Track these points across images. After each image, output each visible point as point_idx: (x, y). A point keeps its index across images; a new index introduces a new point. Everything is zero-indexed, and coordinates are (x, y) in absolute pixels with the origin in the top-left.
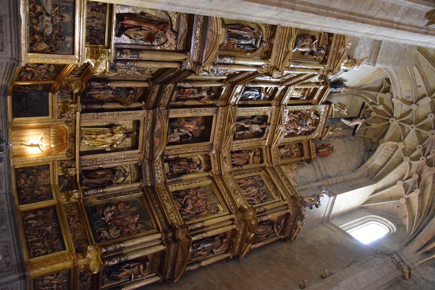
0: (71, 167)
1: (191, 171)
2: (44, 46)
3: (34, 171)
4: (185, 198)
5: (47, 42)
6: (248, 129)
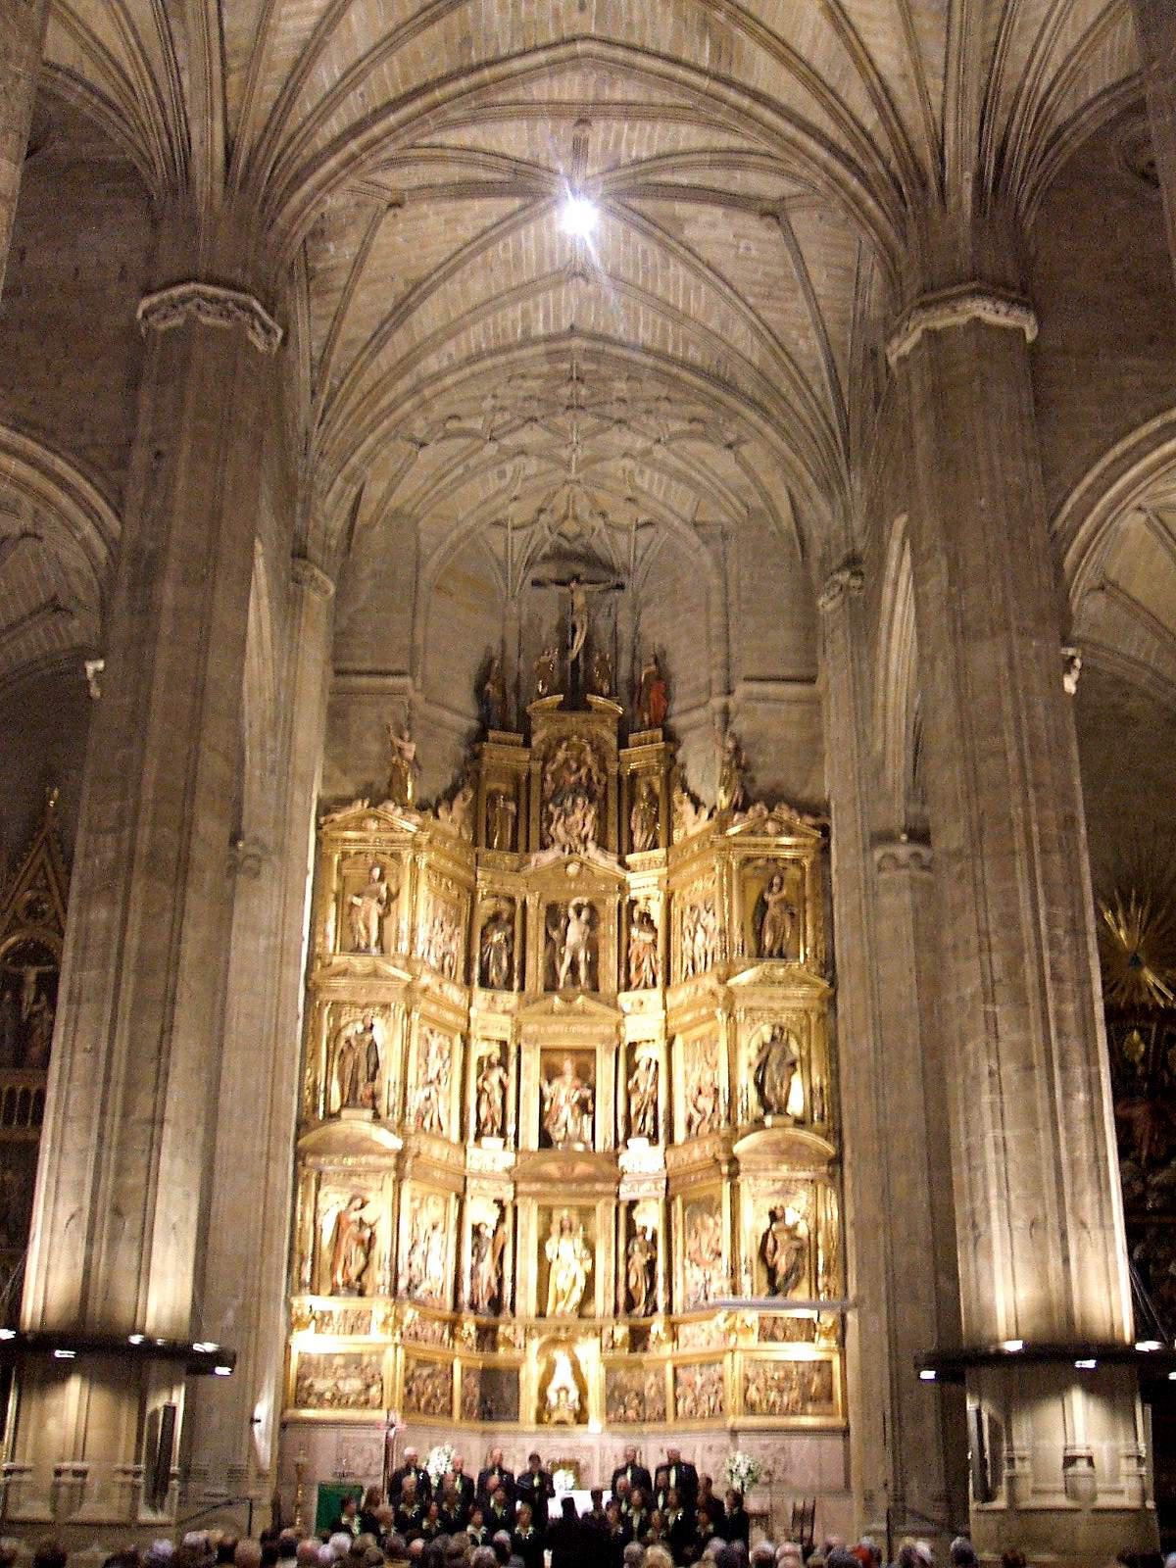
2: (374, 1391)
5: (368, 1387)
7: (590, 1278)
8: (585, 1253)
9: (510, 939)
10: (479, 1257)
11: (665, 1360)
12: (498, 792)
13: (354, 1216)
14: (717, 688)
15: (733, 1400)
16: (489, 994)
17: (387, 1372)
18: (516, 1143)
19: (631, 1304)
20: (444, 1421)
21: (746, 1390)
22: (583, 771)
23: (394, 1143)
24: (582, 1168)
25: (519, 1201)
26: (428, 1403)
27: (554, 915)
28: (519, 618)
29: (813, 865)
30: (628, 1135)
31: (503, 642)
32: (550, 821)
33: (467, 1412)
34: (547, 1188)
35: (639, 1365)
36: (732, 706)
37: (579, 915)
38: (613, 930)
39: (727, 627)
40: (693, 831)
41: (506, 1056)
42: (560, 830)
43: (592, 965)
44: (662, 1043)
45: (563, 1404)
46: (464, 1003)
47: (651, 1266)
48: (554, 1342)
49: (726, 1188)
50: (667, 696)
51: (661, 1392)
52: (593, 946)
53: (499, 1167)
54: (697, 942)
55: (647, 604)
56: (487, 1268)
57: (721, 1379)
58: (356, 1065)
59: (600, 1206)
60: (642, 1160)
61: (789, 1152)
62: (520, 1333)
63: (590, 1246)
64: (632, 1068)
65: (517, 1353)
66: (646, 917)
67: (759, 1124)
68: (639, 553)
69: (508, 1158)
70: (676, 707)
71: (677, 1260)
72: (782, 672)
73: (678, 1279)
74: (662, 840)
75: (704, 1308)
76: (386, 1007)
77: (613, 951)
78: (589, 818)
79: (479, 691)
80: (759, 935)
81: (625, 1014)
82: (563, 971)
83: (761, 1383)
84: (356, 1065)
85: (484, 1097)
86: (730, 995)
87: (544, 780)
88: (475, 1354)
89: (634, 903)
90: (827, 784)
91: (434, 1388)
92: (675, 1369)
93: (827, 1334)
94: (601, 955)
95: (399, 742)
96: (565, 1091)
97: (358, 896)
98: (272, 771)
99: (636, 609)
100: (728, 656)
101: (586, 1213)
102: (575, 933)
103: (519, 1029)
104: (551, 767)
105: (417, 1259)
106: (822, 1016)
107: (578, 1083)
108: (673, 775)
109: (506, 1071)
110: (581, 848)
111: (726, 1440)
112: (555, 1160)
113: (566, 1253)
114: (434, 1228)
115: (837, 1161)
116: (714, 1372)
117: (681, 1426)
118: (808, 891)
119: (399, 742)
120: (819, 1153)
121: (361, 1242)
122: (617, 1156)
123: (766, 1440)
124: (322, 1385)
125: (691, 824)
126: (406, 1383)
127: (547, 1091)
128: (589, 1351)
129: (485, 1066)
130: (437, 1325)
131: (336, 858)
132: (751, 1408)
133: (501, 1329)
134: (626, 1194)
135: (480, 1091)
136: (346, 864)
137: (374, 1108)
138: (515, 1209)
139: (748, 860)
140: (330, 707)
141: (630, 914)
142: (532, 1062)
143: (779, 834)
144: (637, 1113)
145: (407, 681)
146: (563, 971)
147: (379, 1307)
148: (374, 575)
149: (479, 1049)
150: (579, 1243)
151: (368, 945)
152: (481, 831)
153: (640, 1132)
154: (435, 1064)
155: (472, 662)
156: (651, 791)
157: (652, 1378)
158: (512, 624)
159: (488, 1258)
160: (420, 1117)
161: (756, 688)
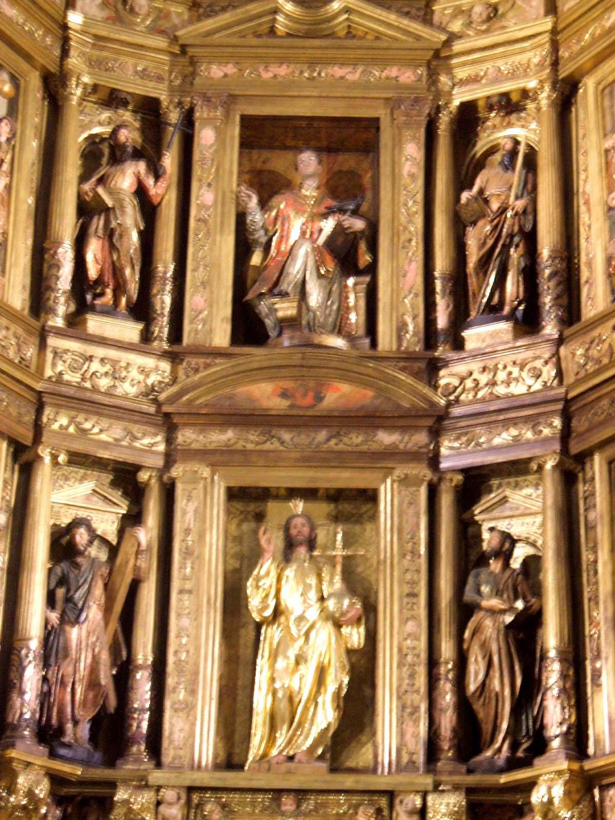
1: (520, 204)
7: (363, 667)
8: (349, 605)
10: (63, 601)
18: (176, 334)
19: (470, 736)
24: (340, 394)
25: (177, 471)
30: (460, 319)
34: (251, 439)
44: (545, 97)
47: (525, 630)
56: (88, 636)
59: (386, 493)
60: (498, 364)
85: (98, 223)
96: (300, 231)
101: (355, 505)
103: (189, 77)
107: (330, 202)
109: (156, 171)
113: (298, 600)
122: (433, 368)
127: (256, 217)
129: (101, 156)
133: (121, 795)
134: (455, 454)
135: (87, 210)
144: (484, 263)
149: (86, 124)
153: (493, 311)
159: (94, 613)
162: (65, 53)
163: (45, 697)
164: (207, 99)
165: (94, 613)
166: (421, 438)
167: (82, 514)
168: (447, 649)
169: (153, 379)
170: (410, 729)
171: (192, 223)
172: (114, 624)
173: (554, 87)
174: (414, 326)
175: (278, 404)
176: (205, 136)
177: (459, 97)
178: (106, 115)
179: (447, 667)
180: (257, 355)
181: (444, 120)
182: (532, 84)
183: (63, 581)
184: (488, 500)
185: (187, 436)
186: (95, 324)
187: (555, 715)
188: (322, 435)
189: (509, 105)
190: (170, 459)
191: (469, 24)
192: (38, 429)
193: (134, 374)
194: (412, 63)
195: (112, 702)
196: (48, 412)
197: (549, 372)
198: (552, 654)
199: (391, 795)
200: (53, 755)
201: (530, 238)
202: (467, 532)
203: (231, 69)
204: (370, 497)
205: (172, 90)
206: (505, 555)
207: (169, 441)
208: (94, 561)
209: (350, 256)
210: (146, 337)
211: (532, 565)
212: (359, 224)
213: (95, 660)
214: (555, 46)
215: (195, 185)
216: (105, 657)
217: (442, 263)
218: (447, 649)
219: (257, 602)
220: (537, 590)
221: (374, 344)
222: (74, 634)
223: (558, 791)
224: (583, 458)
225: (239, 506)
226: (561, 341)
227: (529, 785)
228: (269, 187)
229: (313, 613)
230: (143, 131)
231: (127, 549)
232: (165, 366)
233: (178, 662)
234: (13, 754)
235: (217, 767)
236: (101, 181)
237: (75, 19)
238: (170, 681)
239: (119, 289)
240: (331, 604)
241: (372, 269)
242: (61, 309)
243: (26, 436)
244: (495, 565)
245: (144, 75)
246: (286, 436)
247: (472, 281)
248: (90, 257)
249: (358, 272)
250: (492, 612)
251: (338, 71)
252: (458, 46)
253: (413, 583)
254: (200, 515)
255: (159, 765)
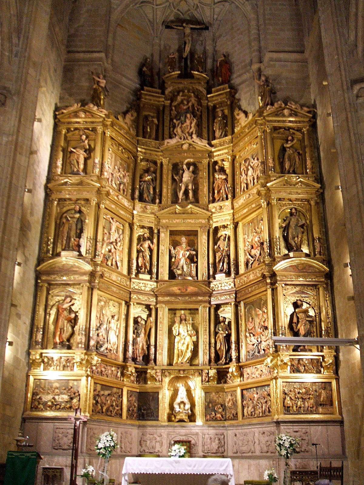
0: (208, 374)
1: (227, 249)
2: (75, 401)
3: (210, 405)
4: (250, 257)
5: (72, 399)
6: (187, 186)
7: (196, 345)
8: (193, 332)
9: (154, 180)
10: (136, 332)
11: (236, 387)
12: (149, 115)
13: (66, 306)
14: (255, 60)
15: (276, 404)
16: (143, 205)
17: (83, 391)
18: (157, 278)
19: (218, 358)
20: (117, 420)
21: (285, 399)
22: (190, 104)
23: (88, 268)
24: (191, 289)
25: (158, 306)
26: (107, 410)
27: (176, 169)
28: (160, 46)
29: (308, 130)
30: (215, 272)
31: (152, 55)
32: (174, 127)
33: (130, 415)
35: (222, 390)
36: (263, 68)
37: (189, 169)
38: (206, 174)
39: (259, 35)
40: (243, 124)
41: (152, 234)
42: (179, 130)
43: (196, 192)
44: (232, 226)
45: (182, 411)
46: (131, 207)
48: (178, 378)
49: (269, 291)
50: (230, 70)
51: (235, 404)
52: (195, 183)
53: (148, 289)
54: (250, 174)
55: (220, 36)
56: (141, 340)
57: (269, 395)
58: (70, 229)
59: (200, 309)
60: (222, 283)
61: (302, 270)
62: (159, 374)
63: (196, 329)
64: (216, 241)
65: (158, 384)
66: (222, 170)
67: (286, 257)
68: (215, 17)
69: (152, 285)
70: (234, 76)
71: (242, 337)
72: (287, 49)
73: (243, 344)
74: (230, 132)
75: (257, 357)
76: (87, 200)
77: (206, 185)
78: (193, 125)
79: (141, 73)
80: (282, 164)
81: (213, 213)
82: (181, 195)
83: (292, 395)
84: (70, 229)
85: (141, 254)
86: (268, 189)
87: (171, 110)
88: (135, 385)
89: (216, 163)
90: (312, 98)
91: (112, 401)
92: (242, 391)
93: (327, 368)
94: (200, 187)
95: (98, 79)
96: (182, 253)
97: (74, 148)
98: (16, 56)
99: (214, 40)
100: (260, 47)
102: (187, 176)
103: (159, 222)
104: (175, 104)
105: (102, 332)
106: (317, 203)
107: (189, 248)
108: (234, 104)
109: (152, 243)
110: (189, 138)
111: (273, 428)
112: (176, 285)
113: (183, 331)
114: (113, 317)
115: (329, 276)
116: (263, 392)
117: (246, 421)
118: (306, 143)
119: (98, 79)
120: (320, 272)
121: (70, 320)
122: (210, 283)
123: (296, 428)
124: (47, 398)
125: (242, 121)
126: (94, 398)
127: (173, 252)
128: (196, 384)
129: (141, 239)
130: (113, 369)
131: (64, 131)
132: (287, 410)
133: (149, 371)
134: (214, 302)
135: (139, 251)
136: (70, 134)
137: (79, 251)
138: (157, 310)
139: (275, 129)
140: (65, 67)
141: (214, 167)
142: (165, 237)
143: (290, 115)
145: (103, 55)
146: (181, 195)
147: (78, 354)
148: (88, 11)
150: (190, 328)
151: (78, 171)
152: (141, 129)
153: (221, 271)
154: (114, 236)
155: (137, 60)
156: (223, 113)
157: (230, 397)
158: (157, 47)
159: (142, 335)
160: (106, 258)
161: (275, 55)
162: (133, 219)
163: (133, 352)
164: (162, 227)
165: (142, 335)
166: (207, 298)
167: (139, 315)
168: (213, 341)
169: (153, 287)
170: (205, 357)
171: (160, 254)
172: (146, 337)
173: (233, 224)
174: (206, 274)
175: (178, 292)
176: (162, 235)
177: (214, 225)
178: (142, 230)
179: (213, 345)
180: (174, 281)
181: (211, 231)
182: (229, 223)
183: (136, 329)
184: (221, 309)
185: (160, 298)
186: (141, 276)
187: (234, 354)
188: (187, 298)
189: (225, 227)
190: (157, 303)
191: (216, 210)
192: (130, 298)
193: (149, 286)
194: (205, 219)
195: (147, 352)
196: (132, 295)
197: (232, 285)
198: (233, 342)
199: (202, 370)
200: (135, 364)
201: (229, 256)
202: (217, 316)
203: (167, 221)
204: (197, 309)
205: (155, 225)
206: (224, 322)
207: (156, 299)
208: (142, 324)
209: (192, 259)
210: (151, 278)
211: (230, 323)
212: (194, 253)
213: (143, 344)
214: (234, 215)
215: (160, 245)
216: (145, 344)
217: (211, 261)
218: (213, 341)
219: (175, 332)
220: (230, 329)
221: (197, 279)
222: (139, 339)
223: (234, 369)
224: (239, 302)
225: (171, 311)
226: (235, 278)
227: (228, 368)
228: (175, 244)
229: (186, 334)
230: (149, 233)
231: (148, 322)
232: (155, 284)
233: (159, 345)
234: (128, 364)
235: (168, 365)
236: (141, 246)
237: (135, 212)
238: (158, 348)
239: (146, 268)
240: (189, 332)
241: (197, 262)
242: (134, 273)
243: (128, 300)
244: (222, 324)
245: (150, 222)
246: (180, 298)
247: (217, 265)
248: (139, 261)
249: (194, 263)
250: (222, 334)
251: (189, 221)
252: (214, 215)
253: (206, 328)
254: (163, 315)
255: (156, 365)
